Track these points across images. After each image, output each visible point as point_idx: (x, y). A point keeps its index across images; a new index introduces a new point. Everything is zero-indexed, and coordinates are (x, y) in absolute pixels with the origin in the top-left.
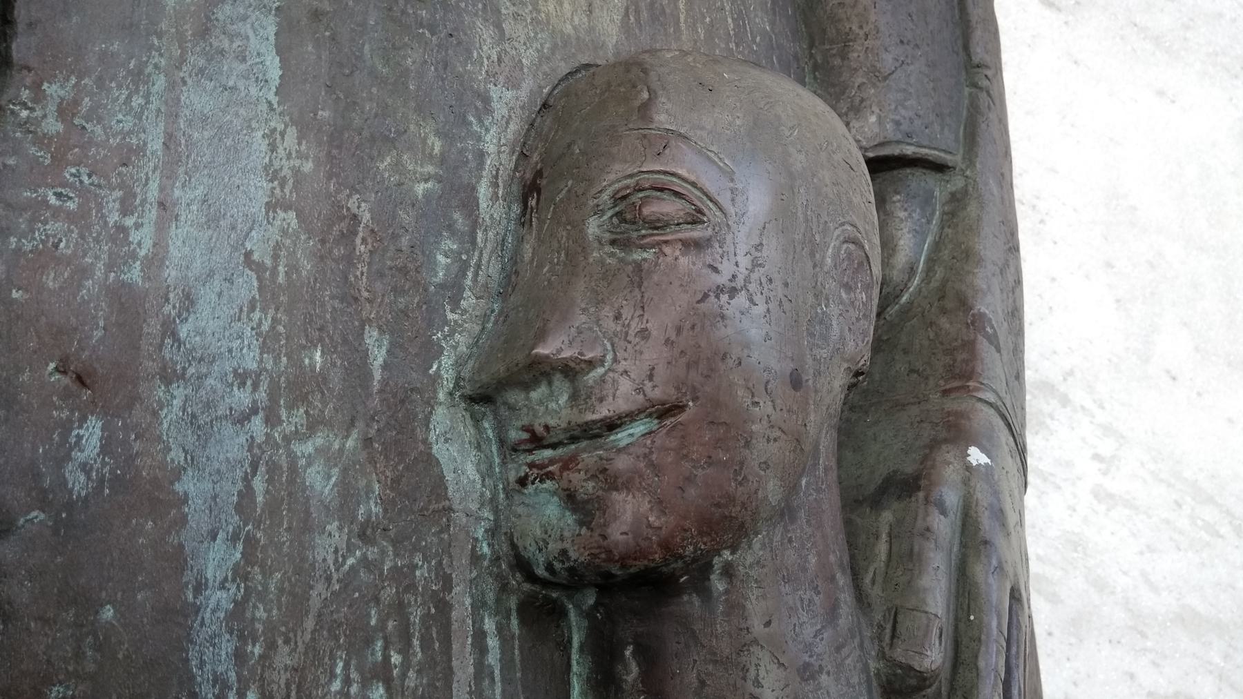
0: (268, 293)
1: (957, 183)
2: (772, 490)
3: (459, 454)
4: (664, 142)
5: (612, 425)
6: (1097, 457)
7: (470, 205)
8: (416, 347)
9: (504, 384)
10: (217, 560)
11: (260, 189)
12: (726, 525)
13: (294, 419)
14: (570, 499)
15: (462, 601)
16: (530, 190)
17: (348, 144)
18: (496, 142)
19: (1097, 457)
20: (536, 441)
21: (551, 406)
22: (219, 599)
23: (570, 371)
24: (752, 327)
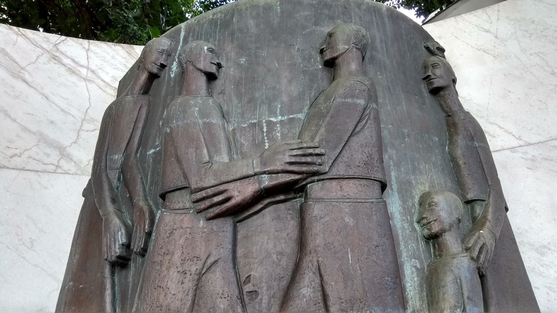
0: (400, 213)
1: (486, 202)
2: (447, 228)
5: (431, 222)
7: (415, 206)
8: (412, 217)
9: (420, 220)
10: (400, 231)
11: (398, 205)
12: (443, 231)
13: (403, 222)
14: (428, 229)
15: (419, 239)
16: (420, 204)
17: (404, 202)
20: (424, 225)
21: (425, 221)
23: (426, 218)
24: (443, 215)
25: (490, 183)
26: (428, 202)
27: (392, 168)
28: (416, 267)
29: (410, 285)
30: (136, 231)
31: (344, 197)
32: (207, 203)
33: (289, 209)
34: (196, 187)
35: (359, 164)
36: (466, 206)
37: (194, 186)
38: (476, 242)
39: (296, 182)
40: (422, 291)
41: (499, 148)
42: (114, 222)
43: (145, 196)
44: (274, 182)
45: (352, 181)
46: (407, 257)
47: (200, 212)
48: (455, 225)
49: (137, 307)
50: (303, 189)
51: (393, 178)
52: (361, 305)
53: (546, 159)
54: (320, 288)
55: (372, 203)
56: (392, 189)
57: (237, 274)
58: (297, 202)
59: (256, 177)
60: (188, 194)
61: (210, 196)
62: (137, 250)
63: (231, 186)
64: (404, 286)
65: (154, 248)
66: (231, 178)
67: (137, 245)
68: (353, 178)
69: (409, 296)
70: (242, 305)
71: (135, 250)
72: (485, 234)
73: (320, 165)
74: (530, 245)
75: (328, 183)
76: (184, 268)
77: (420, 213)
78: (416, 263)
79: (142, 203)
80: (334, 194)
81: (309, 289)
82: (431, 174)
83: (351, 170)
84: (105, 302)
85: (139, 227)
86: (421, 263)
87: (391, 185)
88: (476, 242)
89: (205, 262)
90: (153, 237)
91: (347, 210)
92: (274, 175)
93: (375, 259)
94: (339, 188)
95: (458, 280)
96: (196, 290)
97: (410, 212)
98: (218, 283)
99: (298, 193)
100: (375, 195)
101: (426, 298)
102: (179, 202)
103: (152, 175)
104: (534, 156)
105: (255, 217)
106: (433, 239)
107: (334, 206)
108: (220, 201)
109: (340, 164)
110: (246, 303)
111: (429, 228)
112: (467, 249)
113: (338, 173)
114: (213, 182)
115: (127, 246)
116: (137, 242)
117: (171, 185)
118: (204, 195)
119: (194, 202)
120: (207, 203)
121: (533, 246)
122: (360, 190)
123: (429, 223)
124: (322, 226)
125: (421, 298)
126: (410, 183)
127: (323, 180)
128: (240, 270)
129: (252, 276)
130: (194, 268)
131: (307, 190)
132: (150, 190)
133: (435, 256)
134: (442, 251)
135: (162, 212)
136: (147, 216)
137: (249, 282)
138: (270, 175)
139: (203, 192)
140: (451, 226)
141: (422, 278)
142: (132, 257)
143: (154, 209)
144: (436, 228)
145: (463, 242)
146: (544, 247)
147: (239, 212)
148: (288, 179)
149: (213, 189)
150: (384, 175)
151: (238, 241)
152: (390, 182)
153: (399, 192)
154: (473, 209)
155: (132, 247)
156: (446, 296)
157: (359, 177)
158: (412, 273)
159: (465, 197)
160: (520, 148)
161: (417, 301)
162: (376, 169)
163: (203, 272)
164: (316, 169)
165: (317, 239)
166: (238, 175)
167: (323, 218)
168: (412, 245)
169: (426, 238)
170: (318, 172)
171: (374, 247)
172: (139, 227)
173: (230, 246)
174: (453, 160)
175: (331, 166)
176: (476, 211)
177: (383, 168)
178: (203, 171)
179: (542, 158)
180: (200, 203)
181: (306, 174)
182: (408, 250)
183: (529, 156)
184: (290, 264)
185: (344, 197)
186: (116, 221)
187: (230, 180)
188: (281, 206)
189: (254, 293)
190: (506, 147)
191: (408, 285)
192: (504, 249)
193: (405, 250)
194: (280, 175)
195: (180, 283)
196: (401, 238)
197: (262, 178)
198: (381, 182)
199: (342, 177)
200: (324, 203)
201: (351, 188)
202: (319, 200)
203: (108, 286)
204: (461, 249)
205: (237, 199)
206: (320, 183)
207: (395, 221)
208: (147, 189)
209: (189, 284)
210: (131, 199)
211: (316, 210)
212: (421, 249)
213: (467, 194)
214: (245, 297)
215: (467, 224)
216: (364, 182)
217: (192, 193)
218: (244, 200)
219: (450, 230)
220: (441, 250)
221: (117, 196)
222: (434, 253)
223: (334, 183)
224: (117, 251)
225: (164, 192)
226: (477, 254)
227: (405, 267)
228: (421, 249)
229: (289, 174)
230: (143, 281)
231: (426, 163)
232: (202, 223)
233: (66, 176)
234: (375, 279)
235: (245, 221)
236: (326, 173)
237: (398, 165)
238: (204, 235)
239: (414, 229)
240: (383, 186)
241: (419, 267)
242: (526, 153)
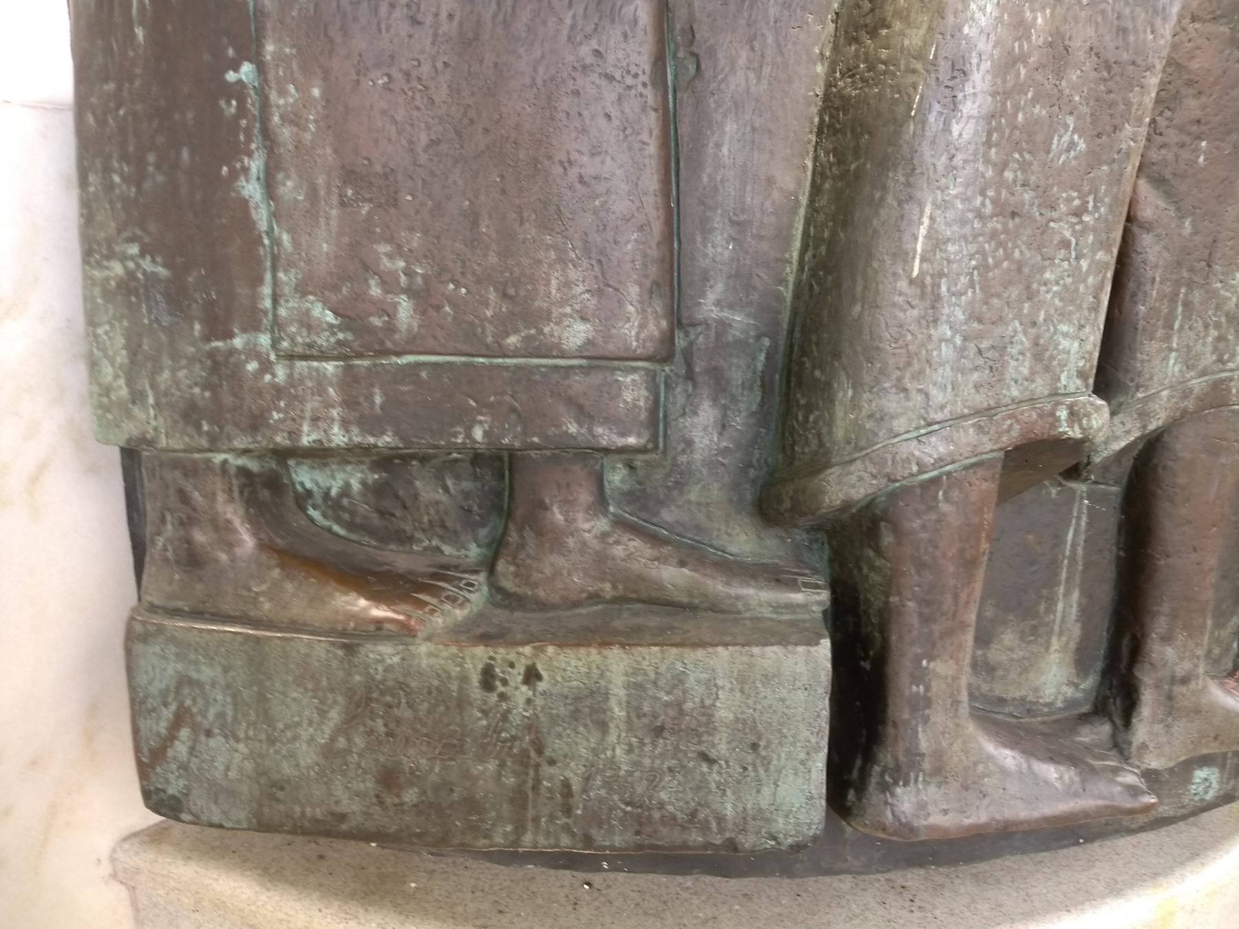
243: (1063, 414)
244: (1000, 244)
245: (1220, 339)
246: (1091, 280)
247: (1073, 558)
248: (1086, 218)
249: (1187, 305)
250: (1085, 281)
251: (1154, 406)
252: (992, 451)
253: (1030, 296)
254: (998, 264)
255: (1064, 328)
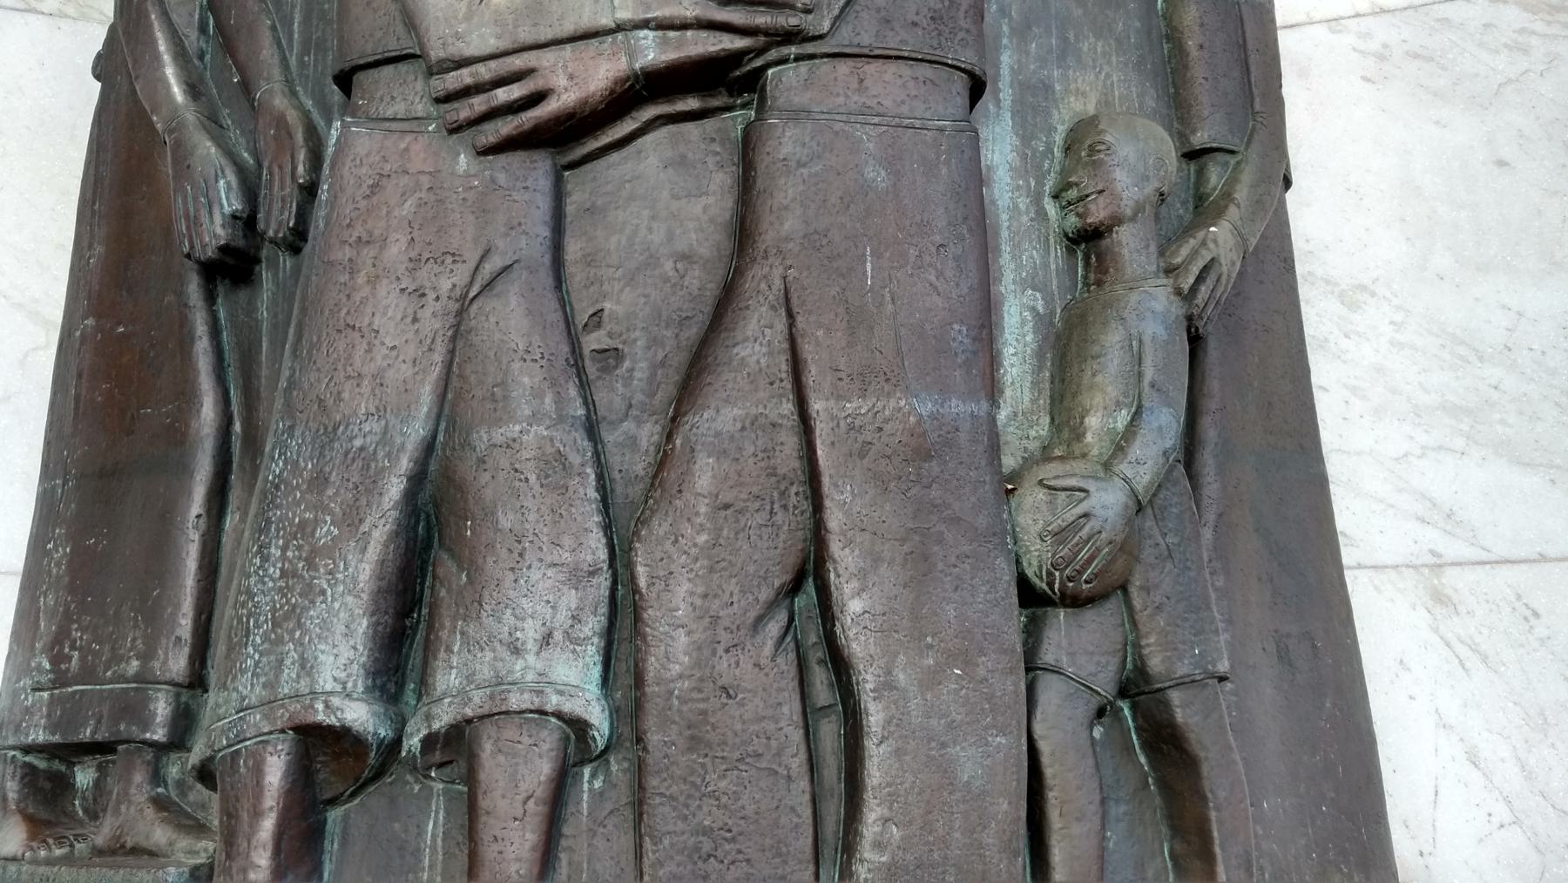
0: (1011, 169)
1: (1239, 157)
2: (1129, 212)
3: (1051, 208)
4: (1102, 131)
6: (1392, 323)
9: (1062, 190)
10: (1004, 217)
12: (1117, 220)
14: (1077, 214)
15: (1052, 241)
16: (1067, 149)
17: (1026, 137)
18: (1059, 139)
19: (1392, 323)
20: (1070, 204)
21: (1073, 194)
22: (1006, 224)
23: (1077, 185)
25: (1257, 107)
26: (1088, 142)
27: (1005, 41)
28: (1033, 309)
29: (1012, 350)
30: (271, 182)
31: (865, 111)
32: (479, 104)
33: (713, 140)
34: (442, 54)
35: (916, 19)
36: (1184, 166)
37: (436, 53)
38: (1194, 253)
39: (736, 57)
40: (1040, 368)
41: (1301, 18)
42: (200, 151)
43: (289, 82)
44: (671, 56)
45: (892, 68)
46: (1014, 282)
47: (456, 129)
48: (1148, 207)
49: (292, 376)
50: (753, 84)
51: (1005, 71)
52: (887, 388)
53: (1416, 56)
54: (786, 345)
55: (941, 130)
56: (998, 102)
57: (564, 303)
58: (736, 121)
59: (620, 36)
60: (420, 77)
61: (485, 84)
62: (276, 232)
63: (545, 59)
64: (999, 353)
65: (327, 224)
66: (547, 34)
67: (277, 218)
68: (898, 58)
69: (1008, 379)
70: (581, 380)
71: (271, 233)
72: (1221, 237)
73: (808, 11)
74: (1328, 282)
75: (825, 66)
76: (418, 283)
77: (1064, 172)
78: (1036, 299)
79: (280, 102)
80: (841, 100)
81: (757, 347)
82: (1106, 69)
83: (891, 34)
84: (196, 372)
85: (276, 170)
86: (1049, 300)
87: (997, 91)
88: (1194, 253)
89: (477, 268)
90: (323, 195)
91: (871, 146)
92: (671, 34)
93: (933, 278)
94: (855, 85)
95: (1134, 343)
96: (454, 339)
97: (1039, 167)
98: (513, 323)
99: (740, 95)
100: (950, 110)
101: (1047, 385)
102: (393, 98)
103: (306, 20)
104: (1385, 46)
105: (615, 157)
106: (1088, 240)
107: (837, 133)
108: (516, 101)
109: (864, 15)
110: (591, 377)
111: (1081, 210)
112: (1170, 271)
113: (856, 41)
114: (492, 44)
115: (247, 222)
116: (275, 212)
117: (366, 46)
118: (468, 81)
119: (438, 101)
120: (479, 104)
121: (1336, 284)
122: (914, 93)
123: (1081, 199)
124: (801, 188)
125: (1035, 384)
126: (1047, 88)
127: (812, 57)
128: (573, 295)
129: (606, 313)
130: (449, 280)
131: (764, 85)
132: (302, 65)
133: (1086, 284)
134: (1106, 272)
135: (345, 126)
136: (299, 137)
137: (599, 325)
138: (660, 33)
139: (465, 71)
140: (1139, 208)
141: (1045, 338)
142: (264, 253)
143: (316, 117)
144: (1098, 213)
145: (1161, 253)
146: (1363, 288)
147: (568, 137)
148: (712, 49)
149: (493, 64)
150: (982, 54)
151: (568, 219)
152: (996, 82)
153: (1019, 114)
154: (1201, 173)
155: (261, 226)
156: (1099, 378)
157: (914, 55)
158: (1023, 322)
159: (1188, 140)
160: (1357, 20)
161: (1027, 392)
162: (961, 35)
163: (472, 295)
164: (793, 21)
165: (786, 217)
166: (568, 28)
167: (804, 165)
168: (1031, 254)
169: (1069, 239)
170: (800, 32)
171: (933, 250)
172: (276, 170)
173: (545, 232)
174: (1173, 36)
175: (837, 18)
176: (1208, 181)
177: (981, 34)
178: (464, 10)
179: (1407, 53)
180: (456, 105)
181: (766, 34)
182: (1019, 267)
183: (1374, 46)
184: (709, 286)
185: (866, 111)
186: (206, 150)
187: (542, 38)
188: (690, 128)
189: (611, 357)
190: (1318, 17)
191: (1008, 351)
192: (1261, 282)
193: (1013, 266)
194: (689, 33)
195: (409, 320)
196: (1005, 234)
197: (639, 39)
198: (970, 74)
199: (866, 51)
200: (809, 124)
201: (888, 86)
202: (797, 115)
203: (201, 328)
204: (1154, 268)
205: (564, 97)
206: (804, 67)
207: (996, 191)
208: (293, 61)
209: (433, 321)
210: (246, 87)
211: (786, 143)
212: (1053, 267)
213: (1194, 132)
214: (588, 363)
215: (1179, 209)
216: (926, 71)
217: (430, 73)
218: (584, 102)
219: (1133, 219)
220: (1102, 269)
221: (202, 80)
222: (1085, 277)
223: (844, 67)
224: (219, 231)
225: (347, 66)
226: (1191, 280)
227: (1006, 308)
228: (1053, 267)
229: (718, 34)
230: (304, 310)
231: (1098, 36)
232: (463, 161)
233: (31, 17)
234: (928, 327)
235: (588, 167)
236: (821, 37)
237: (1022, 32)
238: (471, 195)
239: (1042, 215)
240: (977, 88)
241: (1041, 309)
242: (1367, 35)
243: (320, 706)
244: (285, 595)
245: (495, 659)
246: (342, 615)
247: (433, 848)
248: (340, 576)
249: (462, 633)
250: (336, 615)
251: (436, 710)
252: (271, 733)
253: (299, 625)
254: (282, 607)
255: (321, 647)
